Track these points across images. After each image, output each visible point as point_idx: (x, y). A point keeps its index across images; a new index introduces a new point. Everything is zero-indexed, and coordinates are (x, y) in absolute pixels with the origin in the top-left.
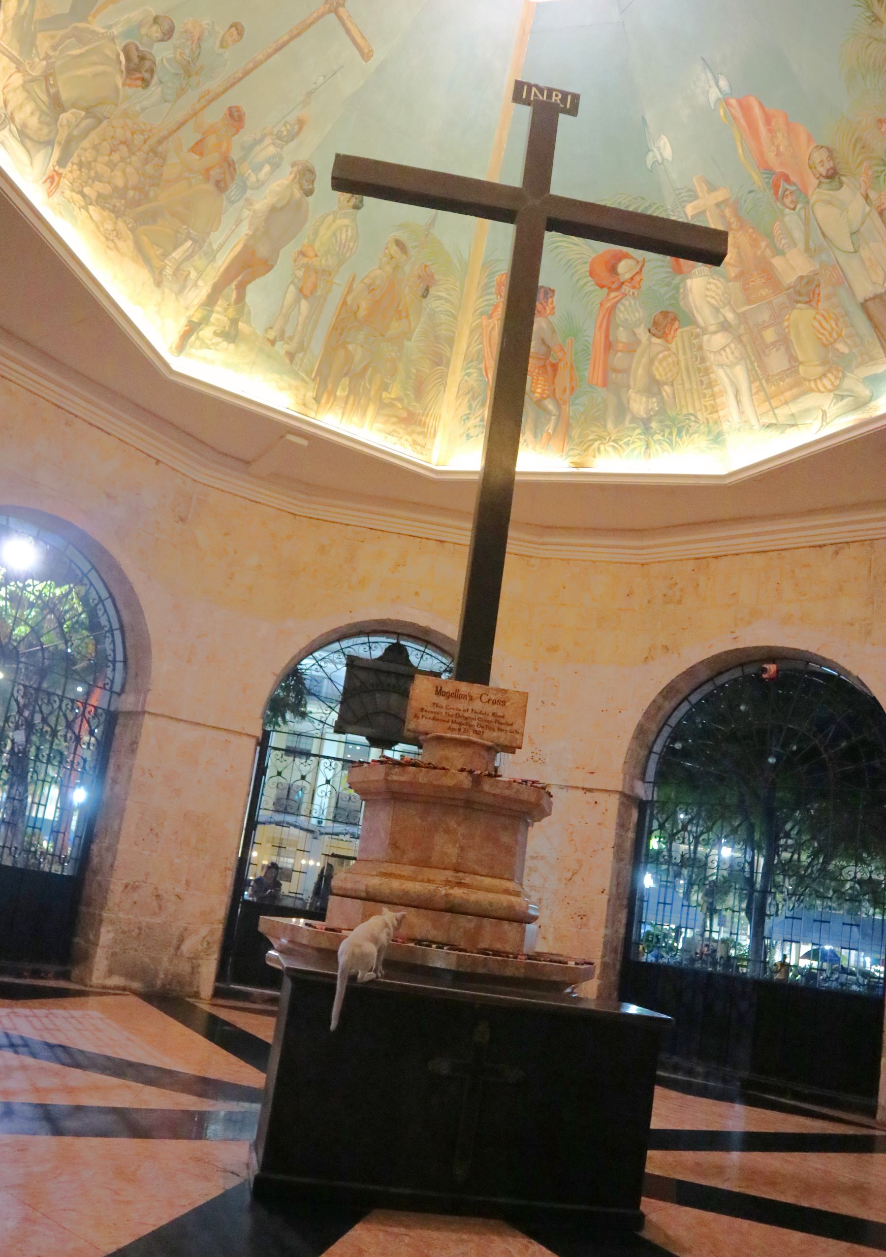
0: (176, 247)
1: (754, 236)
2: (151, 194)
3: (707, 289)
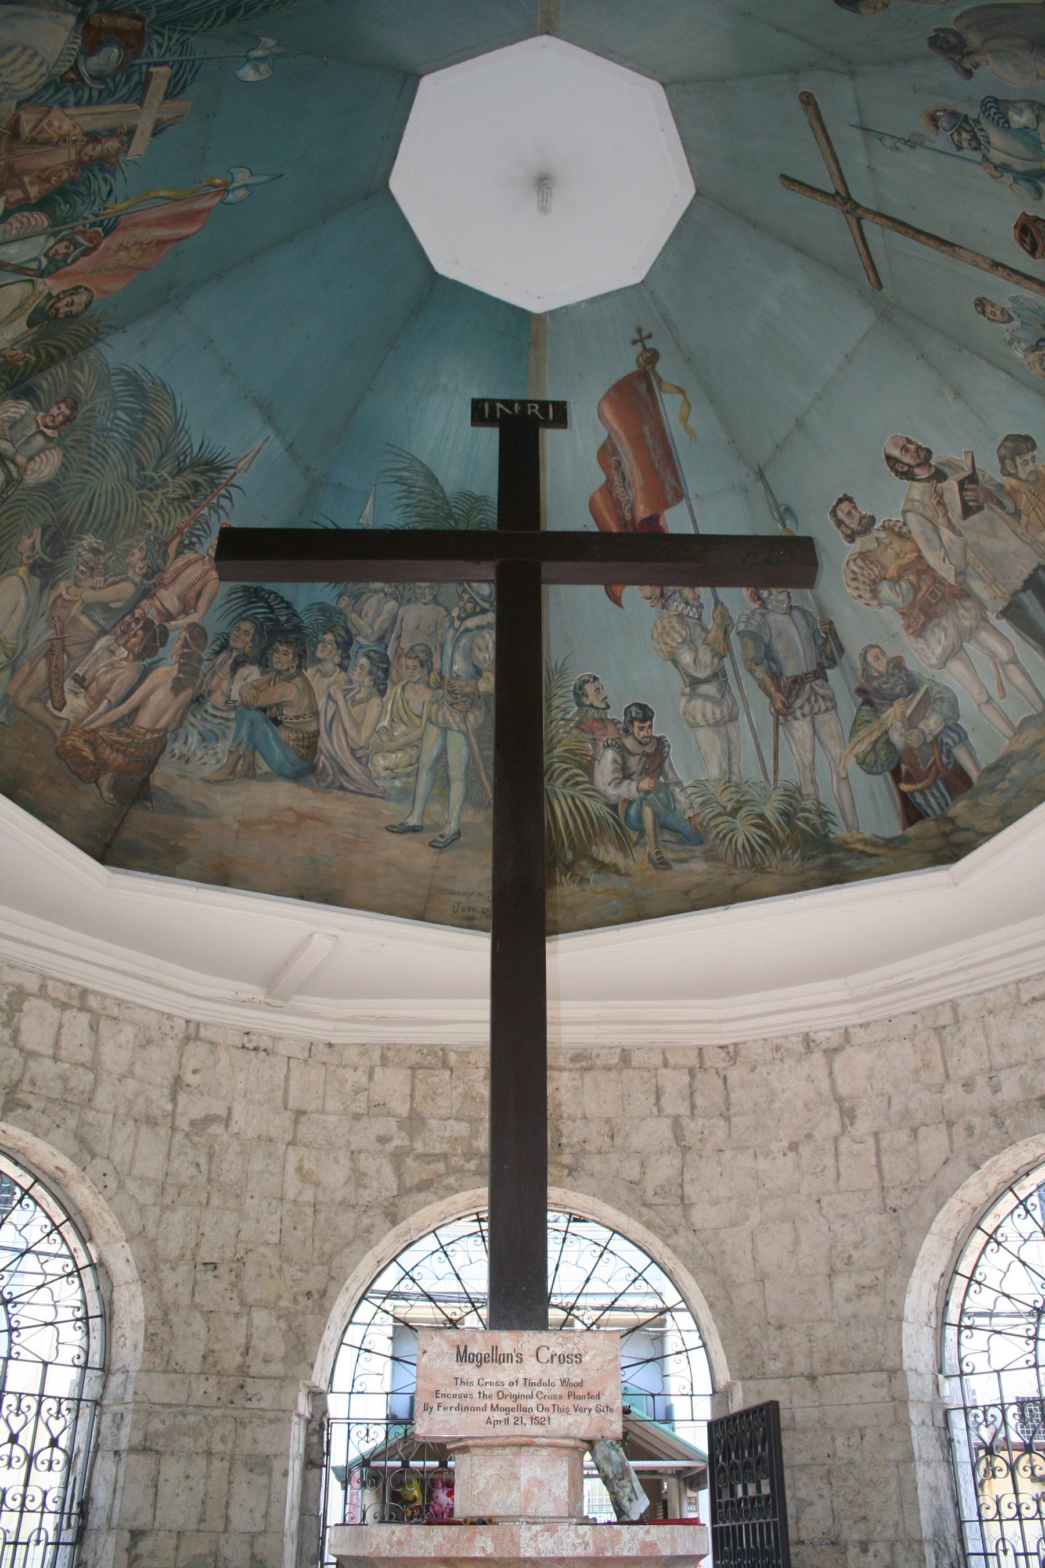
1: (53, 180)
3: (35, 55)
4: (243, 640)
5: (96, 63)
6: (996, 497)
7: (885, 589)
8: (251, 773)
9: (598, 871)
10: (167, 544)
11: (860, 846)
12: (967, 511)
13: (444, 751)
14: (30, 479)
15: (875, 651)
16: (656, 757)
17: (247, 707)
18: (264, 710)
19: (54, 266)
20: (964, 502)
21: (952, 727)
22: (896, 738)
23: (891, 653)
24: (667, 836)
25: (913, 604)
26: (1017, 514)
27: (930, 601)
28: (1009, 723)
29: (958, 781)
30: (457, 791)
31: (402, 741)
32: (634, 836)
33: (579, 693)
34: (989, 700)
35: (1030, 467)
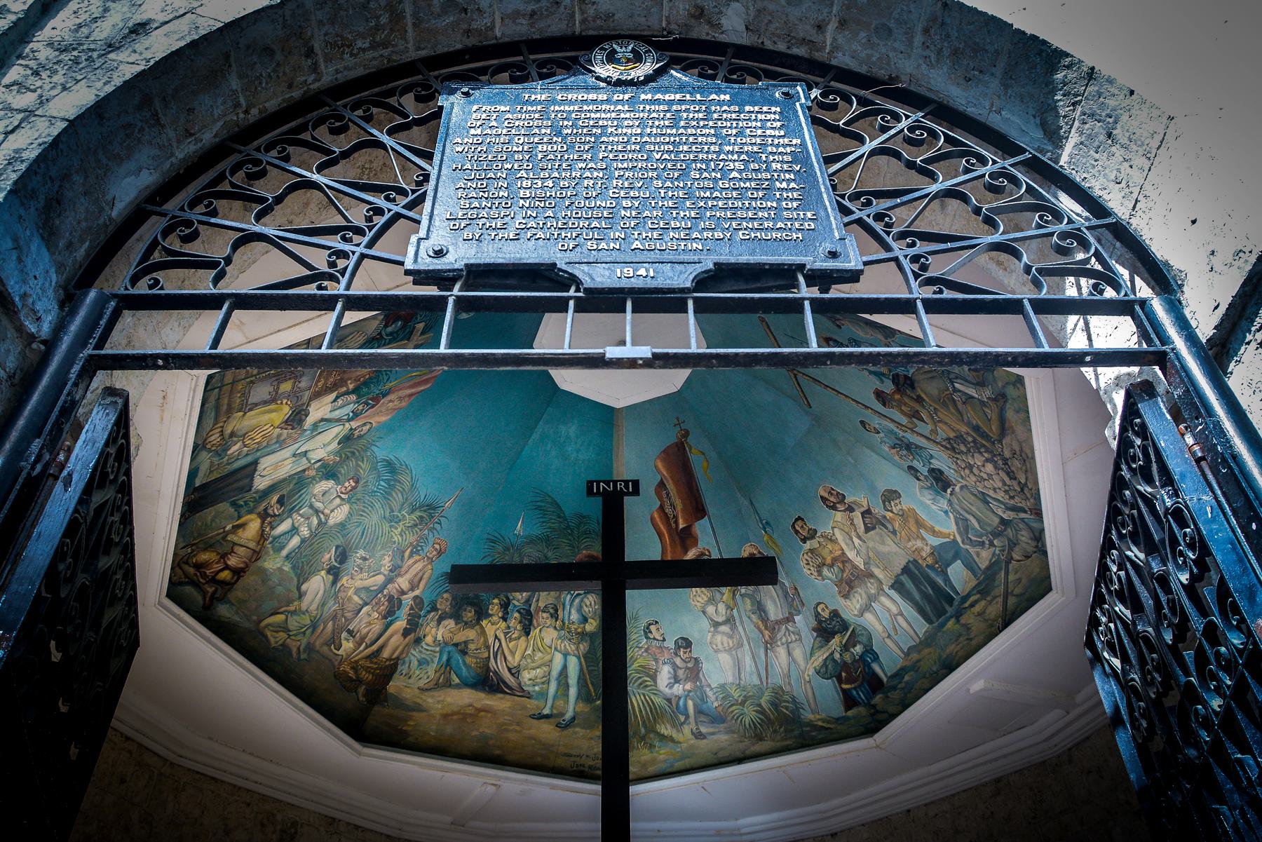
0: (973, 397)
2: (970, 439)
4: (444, 605)
5: (389, 329)
6: (882, 522)
7: (825, 571)
8: (448, 684)
9: (661, 741)
10: (404, 552)
11: (820, 723)
12: (867, 530)
13: (565, 667)
14: (331, 522)
15: (822, 606)
16: (695, 671)
17: (446, 644)
18: (456, 645)
19: (356, 414)
20: (865, 524)
21: (869, 650)
22: (837, 656)
23: (832, 608)
24: (703, 718)
25: (841, 580)
26: (894, 532)
27: (850, 581)
28: (900, 648)
29: (875, 684)
30: (573, 691)
31: (539, 662)
32: (682, 718)
33: (647, 631)
34: (889, 636)
35: (899, 507)
